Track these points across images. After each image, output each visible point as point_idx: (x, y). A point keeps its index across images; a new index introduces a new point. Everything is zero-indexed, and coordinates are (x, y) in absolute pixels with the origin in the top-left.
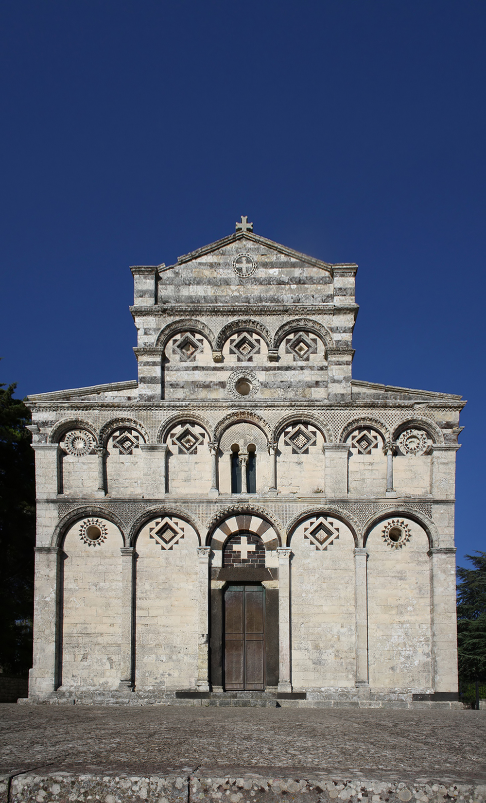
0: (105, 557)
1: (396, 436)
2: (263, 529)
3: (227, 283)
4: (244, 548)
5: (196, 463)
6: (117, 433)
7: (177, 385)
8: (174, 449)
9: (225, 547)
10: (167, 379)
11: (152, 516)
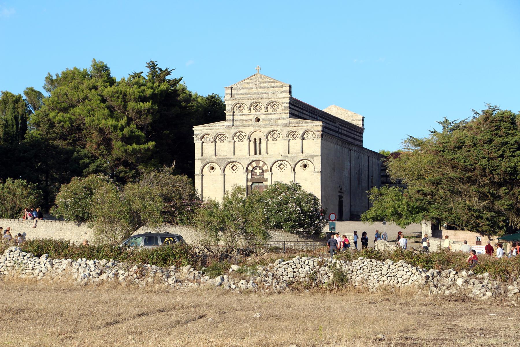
2: (263, 166)
3: (252, 88)
4: (258, 171)
8: (237, 140)
9: (252, 171)
10: (234, 118)
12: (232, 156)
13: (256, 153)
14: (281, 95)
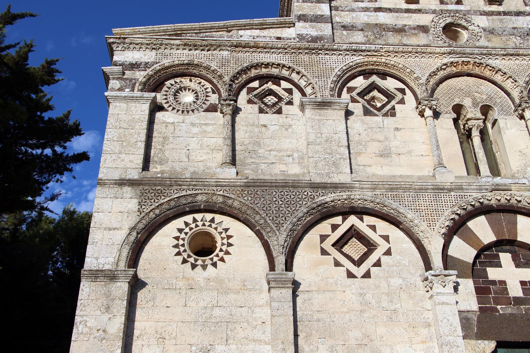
0: (227, 291)
5: (397, 129)
6: (255, 84)
7: (353, 26)
11: (326, 213)
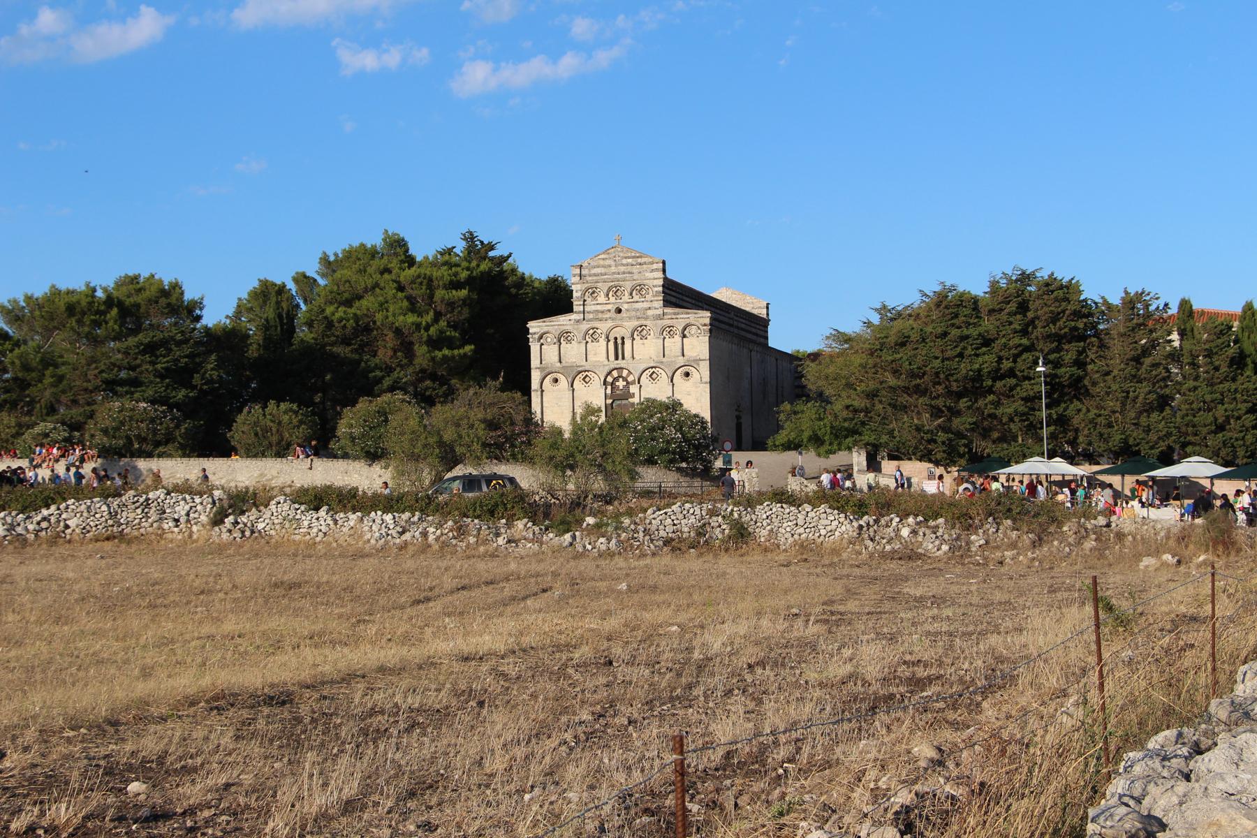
1: (685, 329)
4: (621, 384)
9: (612, 384)
12: (584, 363)
13: (617, 358)
14: (649, 275)
